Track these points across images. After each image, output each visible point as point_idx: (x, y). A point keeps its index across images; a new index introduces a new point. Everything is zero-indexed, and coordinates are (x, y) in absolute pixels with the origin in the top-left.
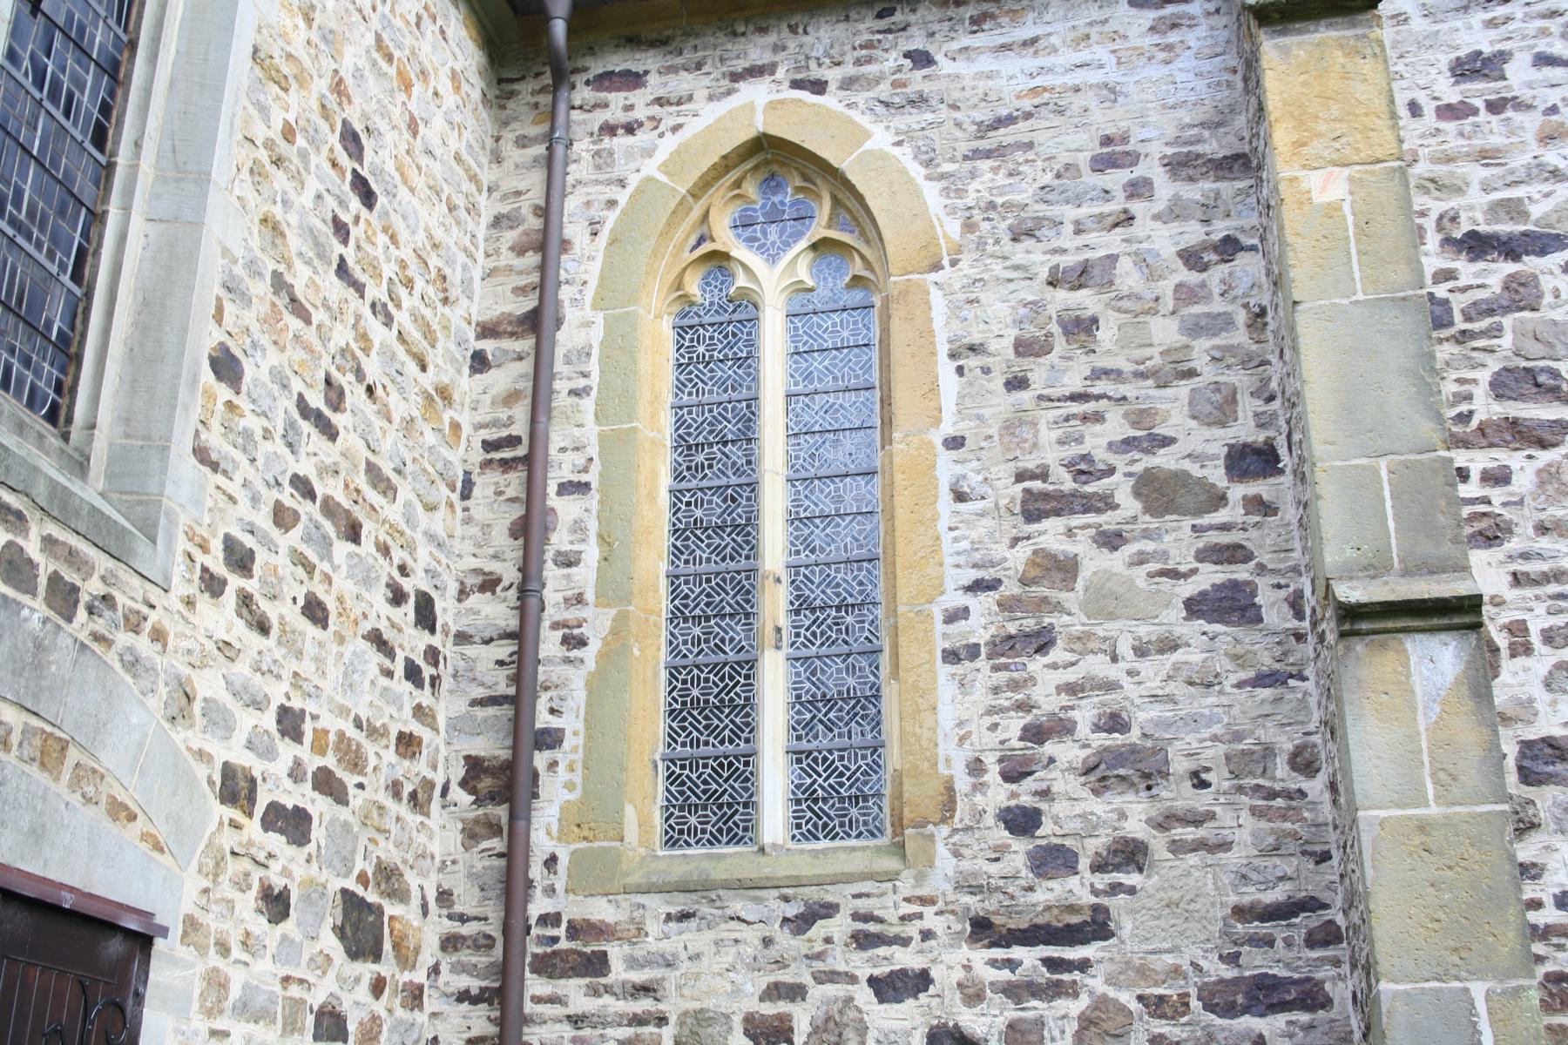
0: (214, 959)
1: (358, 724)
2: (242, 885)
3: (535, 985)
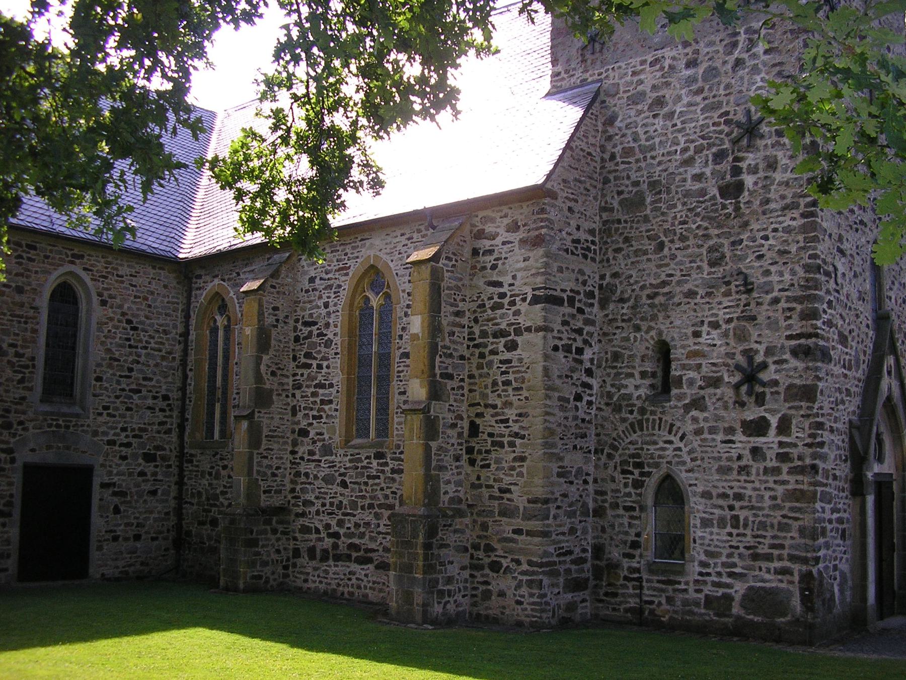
0: (108, 468)
1: (145, 424)
2: (115, 456)
3: (185, 465)
